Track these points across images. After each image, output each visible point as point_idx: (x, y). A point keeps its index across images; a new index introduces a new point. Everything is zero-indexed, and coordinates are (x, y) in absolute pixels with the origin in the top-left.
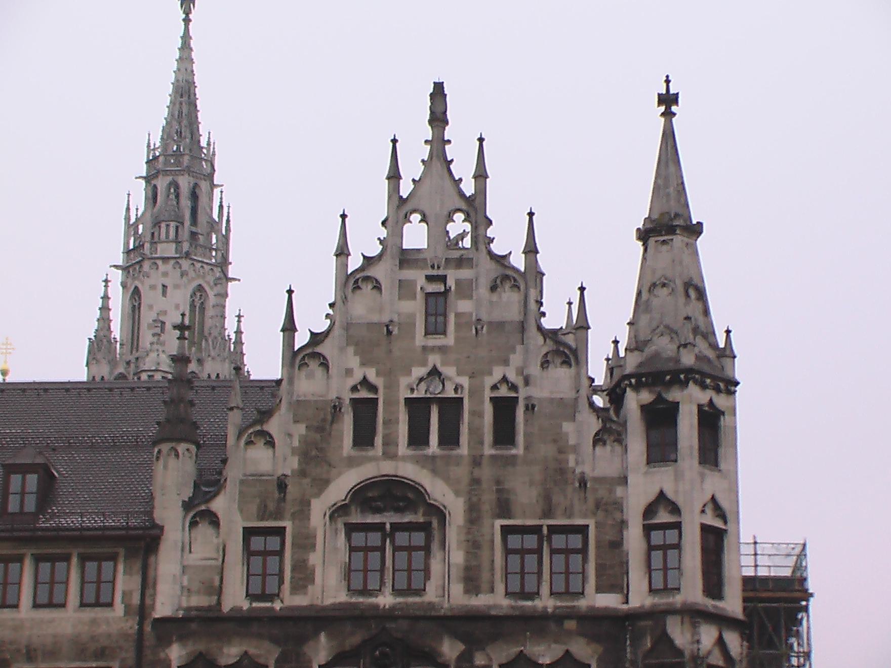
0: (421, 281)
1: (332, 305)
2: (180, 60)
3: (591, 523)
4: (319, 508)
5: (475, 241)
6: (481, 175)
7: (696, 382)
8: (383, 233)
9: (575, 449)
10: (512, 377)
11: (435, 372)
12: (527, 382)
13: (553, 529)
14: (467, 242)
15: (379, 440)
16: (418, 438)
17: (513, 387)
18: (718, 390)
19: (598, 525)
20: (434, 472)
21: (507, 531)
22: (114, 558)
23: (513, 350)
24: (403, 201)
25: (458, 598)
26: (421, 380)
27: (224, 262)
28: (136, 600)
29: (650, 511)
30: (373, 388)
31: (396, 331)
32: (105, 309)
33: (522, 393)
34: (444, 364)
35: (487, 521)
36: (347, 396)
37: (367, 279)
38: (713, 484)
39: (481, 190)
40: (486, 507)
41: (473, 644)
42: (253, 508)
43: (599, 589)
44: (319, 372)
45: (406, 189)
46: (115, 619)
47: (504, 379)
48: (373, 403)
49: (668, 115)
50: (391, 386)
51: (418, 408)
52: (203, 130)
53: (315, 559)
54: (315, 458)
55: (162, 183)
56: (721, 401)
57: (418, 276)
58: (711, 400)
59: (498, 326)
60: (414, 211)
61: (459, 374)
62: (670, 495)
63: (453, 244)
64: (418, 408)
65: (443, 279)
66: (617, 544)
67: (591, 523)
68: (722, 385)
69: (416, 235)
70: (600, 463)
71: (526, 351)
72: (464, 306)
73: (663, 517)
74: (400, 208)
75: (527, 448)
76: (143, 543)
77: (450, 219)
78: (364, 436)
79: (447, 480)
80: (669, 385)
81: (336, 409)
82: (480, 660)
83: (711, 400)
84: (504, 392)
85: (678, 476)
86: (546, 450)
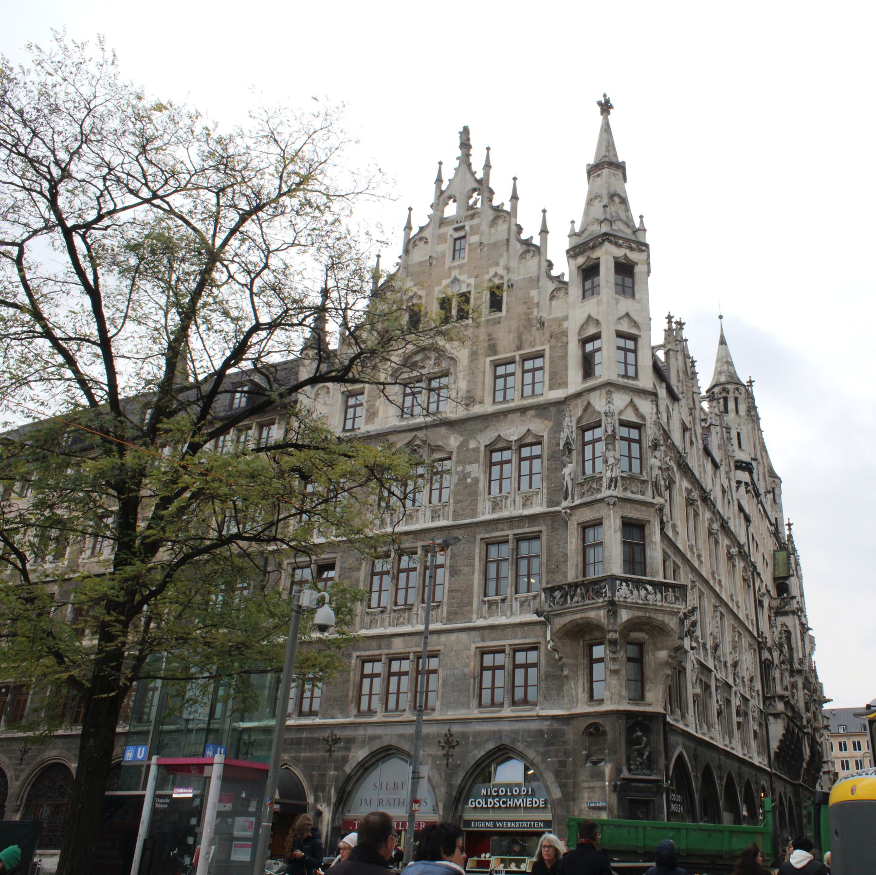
1: (400, 257)
3: (547, 348)
6: (487, 166)
7: (611, 242)
8: (431, 212)
10: (501, 271)
11: (456, 280)
13: (524, 359)
14: (479, 205)
17: (502, 277)
18: (631, 249)
19: (551, 348)
21: (496, 365)
23: (501, 256)
24: (442, 192)
26: (448, 286)
31: (434, 263)
40: (481, 352)
41: (472, 435)
45: (444, 187)
50: (429, 294)
56: (634, 256)
57: (449, 230)
58: (625, 255)
60: (450, 198)
61: (469, 278)
62: (595, 316)
63: (471, 208)
65: (463, 228)
68: (633, 245)
69: (451, 210)
71: (508, 255)
73: (591, 331)
74: (442, 197)
75: (507, 311)
80: (593, 248)
83: (625, 255)
85: (599, 303)
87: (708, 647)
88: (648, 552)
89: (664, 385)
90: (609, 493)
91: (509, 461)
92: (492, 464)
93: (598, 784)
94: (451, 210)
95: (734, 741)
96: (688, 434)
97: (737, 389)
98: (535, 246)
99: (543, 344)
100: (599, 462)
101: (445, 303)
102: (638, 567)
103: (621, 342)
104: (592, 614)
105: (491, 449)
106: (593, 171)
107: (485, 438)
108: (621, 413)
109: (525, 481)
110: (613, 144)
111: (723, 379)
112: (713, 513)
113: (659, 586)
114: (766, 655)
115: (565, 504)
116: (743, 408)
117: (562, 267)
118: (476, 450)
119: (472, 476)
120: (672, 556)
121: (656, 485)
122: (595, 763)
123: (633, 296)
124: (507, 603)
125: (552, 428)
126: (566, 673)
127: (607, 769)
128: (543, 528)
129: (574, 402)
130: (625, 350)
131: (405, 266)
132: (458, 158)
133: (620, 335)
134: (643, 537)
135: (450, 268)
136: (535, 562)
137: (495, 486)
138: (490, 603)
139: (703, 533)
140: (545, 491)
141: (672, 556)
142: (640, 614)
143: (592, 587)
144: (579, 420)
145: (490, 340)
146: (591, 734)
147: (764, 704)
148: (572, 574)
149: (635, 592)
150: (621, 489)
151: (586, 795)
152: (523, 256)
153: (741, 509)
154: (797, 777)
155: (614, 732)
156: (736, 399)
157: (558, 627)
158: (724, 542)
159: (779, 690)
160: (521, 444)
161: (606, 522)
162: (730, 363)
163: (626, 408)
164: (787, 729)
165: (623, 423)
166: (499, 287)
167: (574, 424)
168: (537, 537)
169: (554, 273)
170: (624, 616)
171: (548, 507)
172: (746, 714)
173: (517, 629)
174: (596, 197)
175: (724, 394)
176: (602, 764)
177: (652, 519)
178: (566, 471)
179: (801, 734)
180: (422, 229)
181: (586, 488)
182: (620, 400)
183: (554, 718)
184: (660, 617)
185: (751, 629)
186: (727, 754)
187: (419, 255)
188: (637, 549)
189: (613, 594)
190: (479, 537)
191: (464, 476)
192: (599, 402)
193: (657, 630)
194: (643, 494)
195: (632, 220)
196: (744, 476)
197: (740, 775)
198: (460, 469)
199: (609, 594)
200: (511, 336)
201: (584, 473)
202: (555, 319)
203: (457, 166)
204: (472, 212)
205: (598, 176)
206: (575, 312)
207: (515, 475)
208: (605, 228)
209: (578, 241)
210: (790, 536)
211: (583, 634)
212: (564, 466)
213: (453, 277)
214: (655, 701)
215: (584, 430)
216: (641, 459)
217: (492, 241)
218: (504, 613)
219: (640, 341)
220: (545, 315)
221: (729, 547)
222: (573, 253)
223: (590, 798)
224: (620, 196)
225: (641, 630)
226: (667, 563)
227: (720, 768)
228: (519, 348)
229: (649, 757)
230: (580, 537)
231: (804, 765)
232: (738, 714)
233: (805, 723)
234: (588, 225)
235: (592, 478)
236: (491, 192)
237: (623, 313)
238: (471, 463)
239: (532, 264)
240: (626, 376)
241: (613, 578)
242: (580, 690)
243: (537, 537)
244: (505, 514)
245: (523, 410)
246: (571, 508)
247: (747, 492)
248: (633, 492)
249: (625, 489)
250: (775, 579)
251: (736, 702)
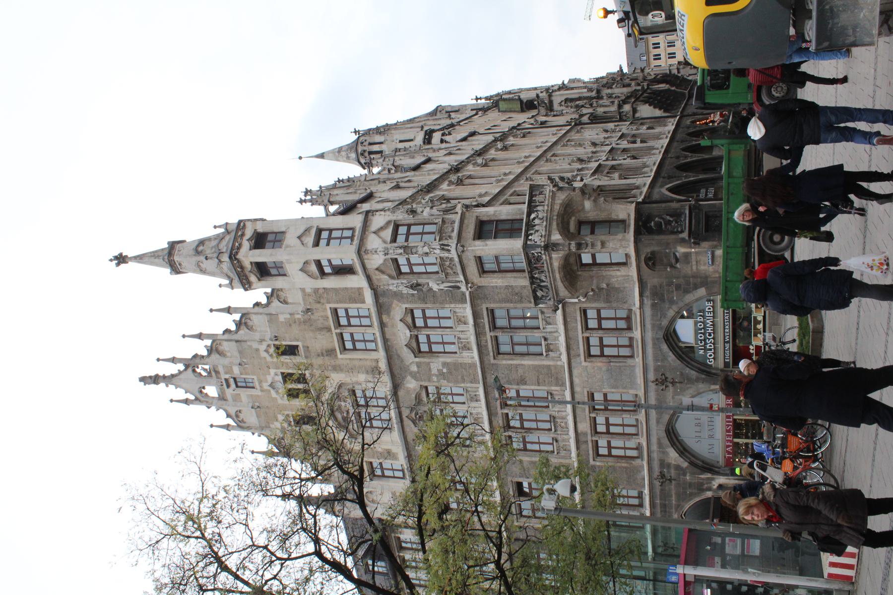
3: (328, 306)
6: (173, 360)
7: (237, 253)
8: (213, 408)
10: (263, 347)
11: (272, 385)
13: (338, 325)
14: (207, 367)
17: (269, 346)
18: (243, 235)
21: (344, 349)
23: (250, 347)
24: (197, 399)
26: (277, 392)
29: (311, 276)
33: (272, 343)
34: (267, 381)
35: (338, 362)
39: (181, 360)
41: (406, 369)
50: (285, 408)
56: (249, 233)
57: (229, 392)
60: (201, 392)
62: (300, 266)
63: (209, 373)
65: (226, 380)
68: (240, 233)
69: (212, 391)
73: (313, 268)
74: (201, 398)
75: (298, 341)
80: (242, 267)
85: (289, 262)
87: (580, 167)
88: (503, 217)
89: (359, 205)
90: (453, 251)
91: (428, 336)
92: (431, 351)
93: (693, 257)
94: (212, 391)
95: (656, 146)
96: (402, 185)
97: (362, 143)
98: (241, 318)
99: (326, 309)
100: (427, 260)
101: (292, 394)
102: (516, 226)
103: (323, 242)
104: (556, 264)
105: (418, 352)
108: (385, 242)
109: (444, 323)
110: (153, 252)
111: (353, 155)
112: (468, 163)
113: (531, 209)
114: (585, 119)
115: (463, 288)
116: (378, 138)
117: (259, 294)
118: (419, 365)
119: (441, 368)
120: (506, 197)
121: (446, 211)
122: (677, 260)
123: (283, 233)
124: (548, 336)
125: (399, 301)
126: (604, 286)
127: (681, 250)
128: (484, 307)
129: (375, 282)
130: (329, 239)
131: (260, 429)
132: (167, 386)
133: (316, 244)
134: (490, 222)
135: (262, 391)
136: (513, 313)
137: (449, 348)
138: (548, 350)
139: (486, 171)
140: (453, 306)
141: (506, 197)
142: (555, 223)
143: (533, 264)
144: (392, 277)
145: (323, 355)
146: (654, 264)
147: (625, 121)
148: (522, 282)
149: (537, 228)
150: (450, 241)
151: (702, 268)
152: (250, 328)
153: (464, 139)
154: (684, 94)
155: (652, 245)
156: (370, 144)
157: (567, 292)
158: (492, 153)
159: (614, 108)
160: (413, 326)
161: (478, 254)
162: (340, 150)
163: (380, 237)
164: (645, 102)
165: (394, 239)
166: (277, 348)
167: (395, 282)
168: (491, 312)
169: (264, 301)
170: (556, 237)
171: (466, 303)
172: (634, 136)
173: (570, 327)
174: (199, 266)
175: (366, 154)
176: (677, 254)
177: (475, 214)
178: (435, 287)
179: (649, 91)
180: (228, 416)
181: (449, 271)
182: (373, 242)
183: (641, 295)
184: (557, 207)
185: (564, 132)
186: (666, 151)
187: (251, 417)
188: (501, 227)
189: (539, 246)
190: (492, 361)
191: (441, 374)
192: (376, 261)
193: (568, 210)
194: (453, 222)
195: (218, 235)
196: (437, 137)
197: (682, 141)
198: (435, 379)
199: (539, 250)
200: (319, 336)
201: (437, 273)
202: (304, 300)
203: (173, 387)
204: (213, 373)
205: (180, 264)
206: (297, 283)
207: (439, 331)
208: (225, 258)
209: (236, 281)
210: (487, 98)
211: (573, 271)
212: (431, 289)
213: (269, 388)
214: (626, 211)
215: (400, 273)
216: (424, 224)
217: (238, 355)
218: (557, 338)
219: (322, 226)
220: (301, 308)
221: (497, 150)
222: (247, 285)
223: (705, 264)
224: (198, 246)
225: (568, 223)
226: (512, 201)
227: (678, 157)
228: (329, 330)
229: (671, 216)
230: (491, 275)
231: (673, 88)
232: (634, 142)
233: (639, 88)
234: (222, 272)
235: (442, 265)
236: (195, 356)
237: (298, 241)
238: (430, 369)
239: (257, 320)
240: (352, 238)
241: (525, 246)
242: (618, 273)
243: (492, 311)
244: (473, 339)
245: (382, 325)
246: (467, 283)
247: (450, 134)
248: (453, 231)
249: (450, 237)
250: (522, 111)
251: (624, 144)
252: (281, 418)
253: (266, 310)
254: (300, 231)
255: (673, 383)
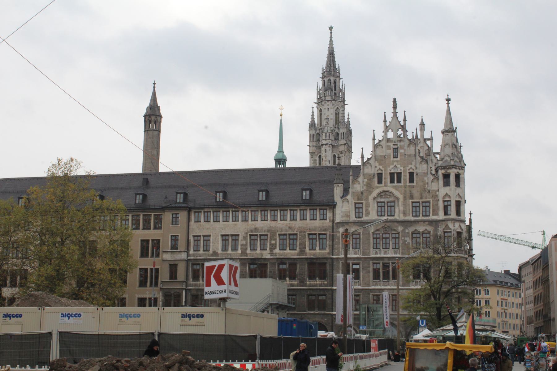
0: (392, 145)
2: (330, 44)
3: (431, 200)
4: (371, 198)
5: (404, 136)
6: (405, 120)
8: (383, 134)
9: (428, 183)
10: (413, 167)
12: (416, 168)
14: (402, 136)
15: (383, 182)
16: (392, 181)
17: (413, 170)
20: (396, 189)
21: (412, 202)
22: (326, 209)
24: (387, 127)
25: (402, 218)
27: (344, 101)
28: (332, 219)
29: (444, 197)
30: (382, 170)
32: (313, 115)
36: (376, 172)
37: (380, 145)
38: (458, 190)
39: (405, 124)
41: (406, 227)
42: (356, 198)
43: (433, 215)
44: (370, 167)
45: (388, 124)
46: (327, 223)
47: (411, 168)
48: (382, 174)
49: (448, 103)
50: (386, 170)
51: (392, 175)
52: (337, 63)
53: (370, 209)
54: (369, 186)
55: (326, 79)
56: (460, 172)
57: (391, 144)
59: (410, 156)
62: (449, 194)
63: (399, 136)
64: (392, 175)
65: (397, 145)
66: (437, 204)
67: (431, 200)
69: (390, 135)
70: (433, 186)
71: (416, 162)
72: (402, 151)
73: (447, 199)
74: (387, 128)
76: (332, 206)
77: (398, 131)
78: (380, 181)
79: (399, 191)
80: (448, 169)
81: (374, 175)
82: (407, 231)
84: (411, 171)
85: (450, 190)
86: (421, 184)
105: (413, 233)
106: (444, 132)
107: (411, 229)
118: (408, 233)
144: (444, 229)
160: (423, 233)
166: (413, 173)
191: (405, 241)
192: (451, 225)
198: (403, 238)
202: (434, 190)
217: (409, 154)
228: (421, 198)
245: (424, 221)
252: (381, 167)
253: (429, 173)
254: (461, 195)
255: (405, 324)
